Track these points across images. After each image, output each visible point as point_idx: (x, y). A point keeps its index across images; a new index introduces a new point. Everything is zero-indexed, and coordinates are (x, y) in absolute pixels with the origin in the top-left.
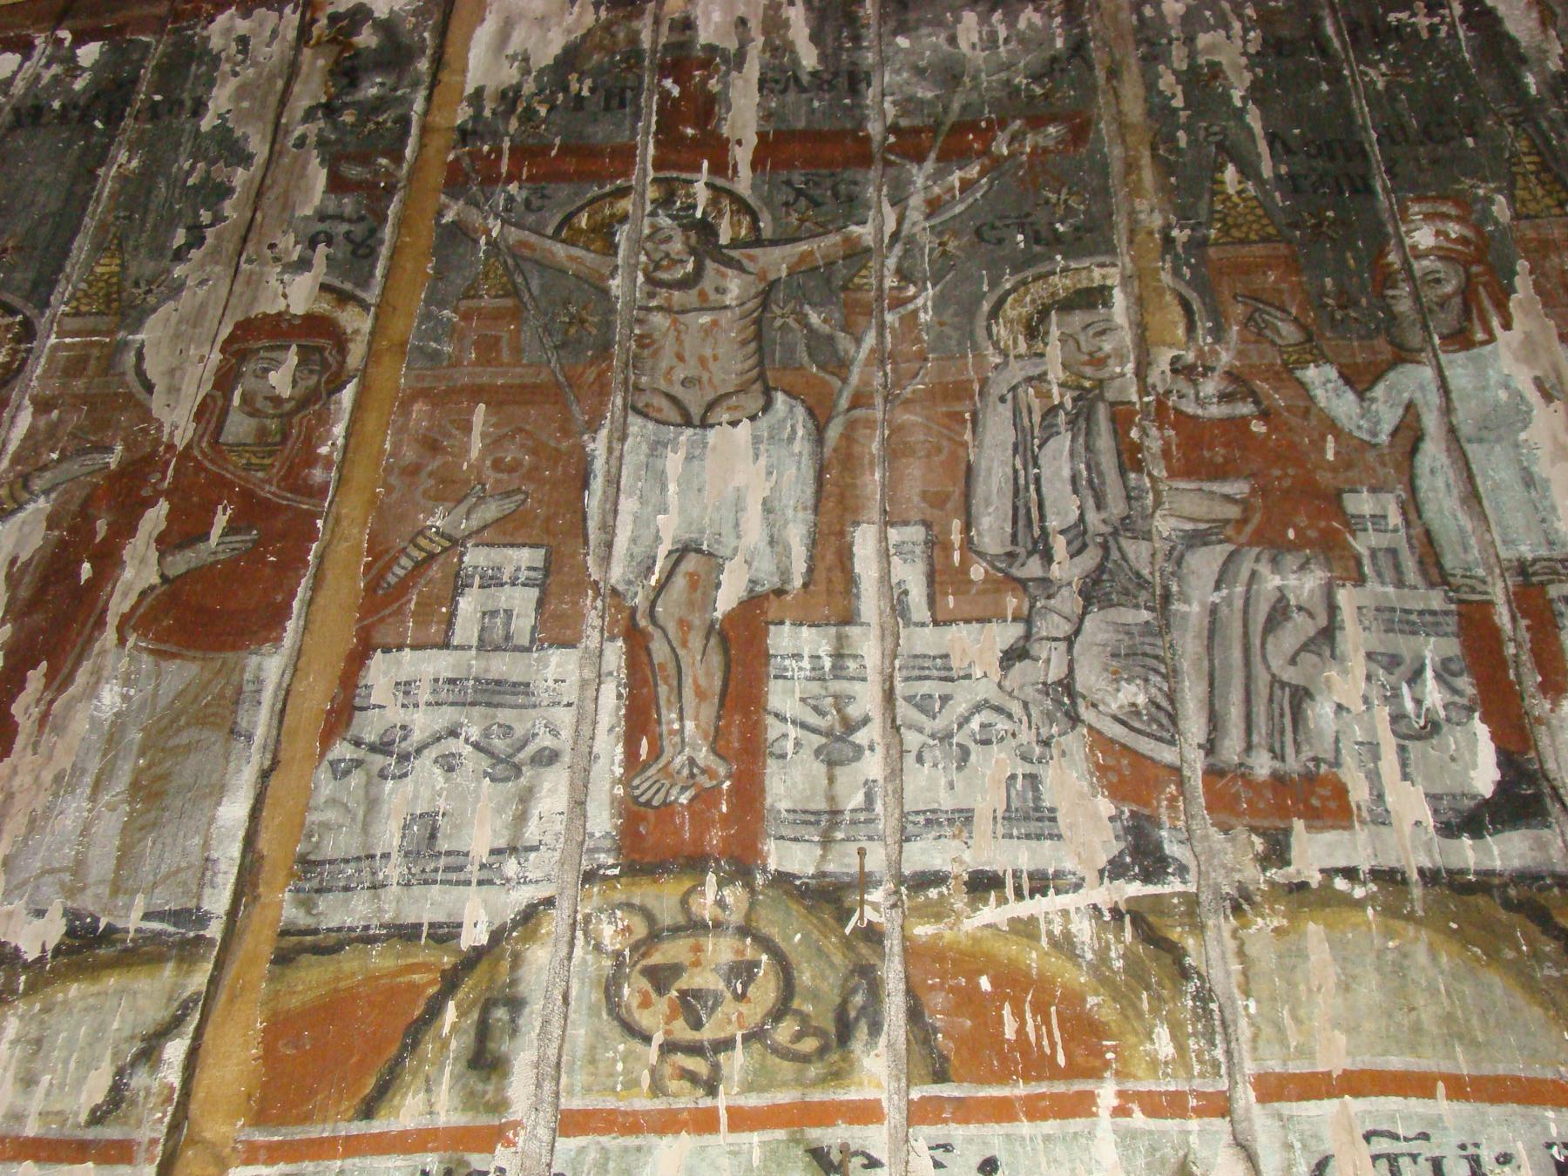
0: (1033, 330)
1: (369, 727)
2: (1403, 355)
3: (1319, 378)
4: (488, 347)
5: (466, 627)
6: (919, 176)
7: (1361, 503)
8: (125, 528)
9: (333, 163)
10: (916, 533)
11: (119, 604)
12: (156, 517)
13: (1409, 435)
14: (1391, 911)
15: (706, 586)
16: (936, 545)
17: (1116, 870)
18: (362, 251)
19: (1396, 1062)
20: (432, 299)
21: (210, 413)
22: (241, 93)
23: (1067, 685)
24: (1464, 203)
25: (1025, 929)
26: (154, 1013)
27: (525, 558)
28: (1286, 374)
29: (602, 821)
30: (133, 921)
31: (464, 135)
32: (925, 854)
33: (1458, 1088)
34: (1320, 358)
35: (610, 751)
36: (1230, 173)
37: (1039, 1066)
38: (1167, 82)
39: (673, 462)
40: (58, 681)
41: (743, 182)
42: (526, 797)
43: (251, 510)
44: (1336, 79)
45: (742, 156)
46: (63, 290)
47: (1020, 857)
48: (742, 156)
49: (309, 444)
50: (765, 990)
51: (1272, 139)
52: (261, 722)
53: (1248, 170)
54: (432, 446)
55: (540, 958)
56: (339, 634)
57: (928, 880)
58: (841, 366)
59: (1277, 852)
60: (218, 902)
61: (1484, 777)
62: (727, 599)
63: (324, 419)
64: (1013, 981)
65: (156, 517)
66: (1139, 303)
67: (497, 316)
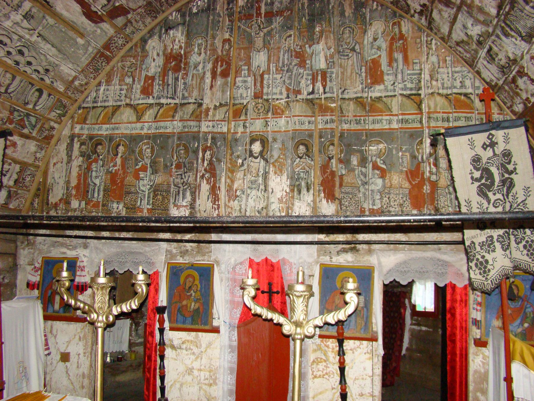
0: (286, 40)
1: (237, 85)
2: (314, 44)
3: (307, 46)
4: (243, 42)
5: (243, 75)
6: (278, 18)
7: (308, 62)
8: (218, 65)
9: (229, 17)
10: (274, 65)
11: (218, 73)
12: (219, 63)
13: (313, 53)
14: (303, 102)
15: (260, 70)
16: (276, 66)
17: (286, 98)
18: (232, 29)
19: (301, 114)
20: (238, 36)
21: (222, 51)
22: (220, 7)
23: (284, 81)
24: (321, 24)
25: (280, 103)
26: (226, 110)
27: (247, 67)
28: (304, 46)
29: (253, 94)
30: (223, 103)
31: (240, 13)
32: (274, 97)
33: (304, 116)
34: (308, 44)
35: (253, 87)
36: (304, 19)
37: (280, 114)
38: (300, 5)
39: (257, 56)
40: (215, 81)
41: (263, 20)
42: (248, 92)
43: (227, 63)
44: (315, 4)
45: (263, 15)
46: (209, 36)
47: (279, 97)
48: (263, 15)
49: (230, 55)
50: (263, 108)
51: (308, 13)
52: (229, 85)
53: (305, 18)
54: (239, 55)
55: (249, 106)
56: (234, 76)
57: (274, 99)
58: (270, 44)
59: (296, 97)
60: (228, 101)
61: (311, 90)
62: (261, 72)
63: (230, 52)
64: (279, 108)
65: (219, 63)
66: (294, 37)
67: (243, 38)
